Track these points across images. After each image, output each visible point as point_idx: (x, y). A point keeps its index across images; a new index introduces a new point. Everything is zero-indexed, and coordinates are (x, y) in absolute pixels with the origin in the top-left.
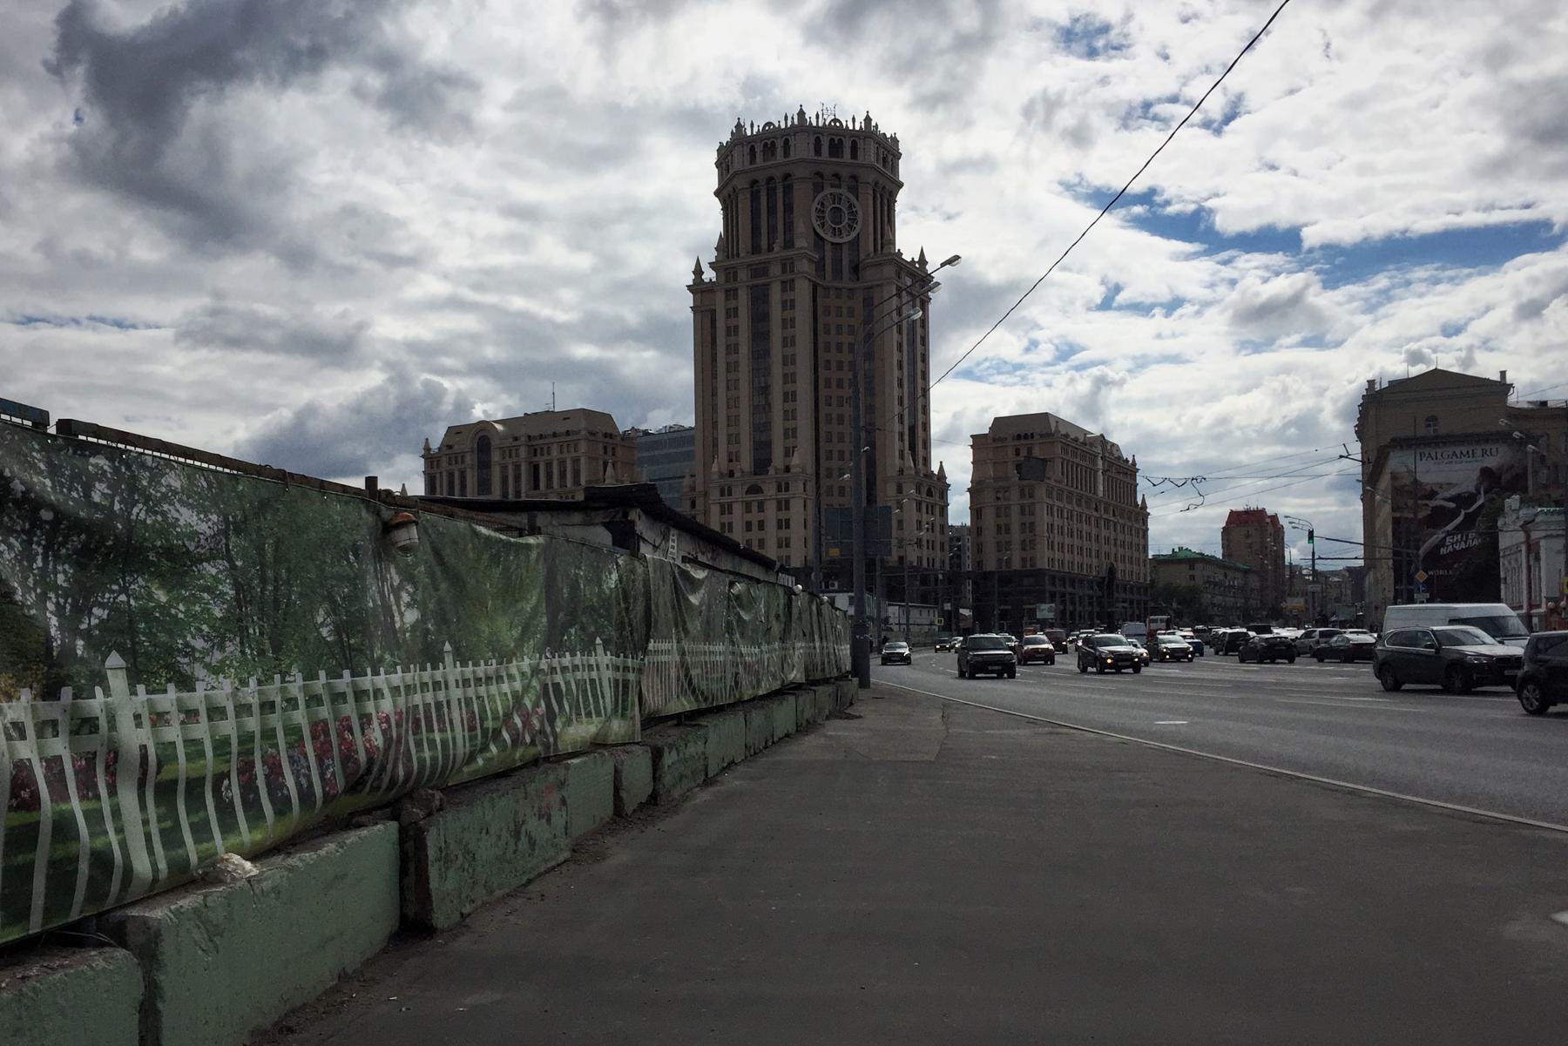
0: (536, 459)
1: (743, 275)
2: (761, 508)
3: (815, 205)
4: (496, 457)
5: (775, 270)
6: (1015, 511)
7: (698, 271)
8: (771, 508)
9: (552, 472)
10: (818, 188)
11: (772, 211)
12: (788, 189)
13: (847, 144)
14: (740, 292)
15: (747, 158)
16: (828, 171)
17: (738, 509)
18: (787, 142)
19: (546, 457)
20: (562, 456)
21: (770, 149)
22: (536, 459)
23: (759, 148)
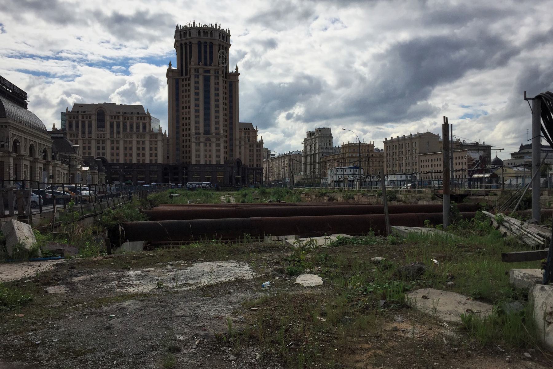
1: (201, 71)
3: (219, 54)
4: (108, 118)
5: (213, 72)
8: (214, 145)
11: (205, 52)
12: (211, 47)
13: (225, 36)
14: (200, 76)
15: (197, 34)
17: (202, 145)
18: (211, 32)
22: (125, 121)
23: (202, 32)
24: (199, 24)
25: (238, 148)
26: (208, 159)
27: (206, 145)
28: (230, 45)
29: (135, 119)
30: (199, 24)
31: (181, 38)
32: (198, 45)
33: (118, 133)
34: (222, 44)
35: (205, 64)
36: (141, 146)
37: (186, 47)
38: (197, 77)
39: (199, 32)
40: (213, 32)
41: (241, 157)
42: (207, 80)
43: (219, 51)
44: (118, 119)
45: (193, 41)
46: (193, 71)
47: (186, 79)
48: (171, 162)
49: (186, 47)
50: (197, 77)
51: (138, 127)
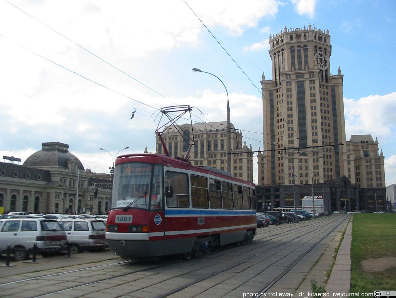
0: (210, 139)
1: (293, 77)
2: (306, 161)
3: (315, 56)
5: (307, 76)
6: (373, 167)
7: (264, 77)
8: (310, 161)
9: (211, 145)
10: (316, 51)
11: (299, 57)
12: (306, 50)
13: (323, 38)
15: (289, 39)
16: (319, 46)
18: (305, 35)
19: (214, 138)
21: (298, 36)
23: (294, 36)
24: (291, 29)
25: (345, 163)
26: (304, 179)
27: (301, 161)
29: (219, 136)
30: (291, 29)
31: (274, 47)
32: (291, 51)
33: (202, 152)
38: (289, 83)
39: (292, 38)
40: (307, 34)
41: (349, 176)
43: (315, 54)
44: (202, 137)
48: (267, 182)
50: (289, 83)
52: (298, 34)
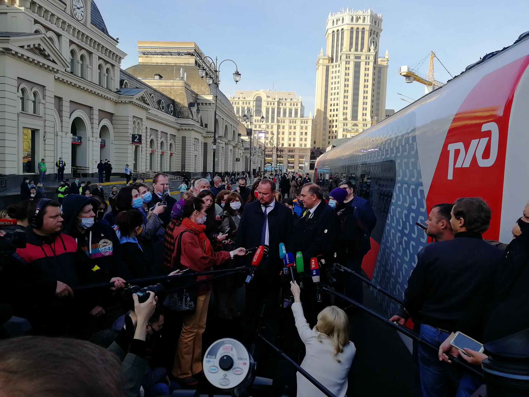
1: (352, 57)
4: (264, 105)
11: (357, 38)
13: (377, 22)
20: (291, 107)
28: (382, 30)
29: (288, 105)
31: (333, 25)
32: (351, 31)
33: (273, 118)
34: (374, 29)
35: (356, 50)
36: (292, 131)
37: (338, 34)
38: (347, 63)
40: (366, 17)
42: (357, 66)
43: (370, 36)
45: (345, 27)
46: (344, 57)
47: (336, 66)
49: (338, 34)
51: (290, 113)
52: (358, 16)
